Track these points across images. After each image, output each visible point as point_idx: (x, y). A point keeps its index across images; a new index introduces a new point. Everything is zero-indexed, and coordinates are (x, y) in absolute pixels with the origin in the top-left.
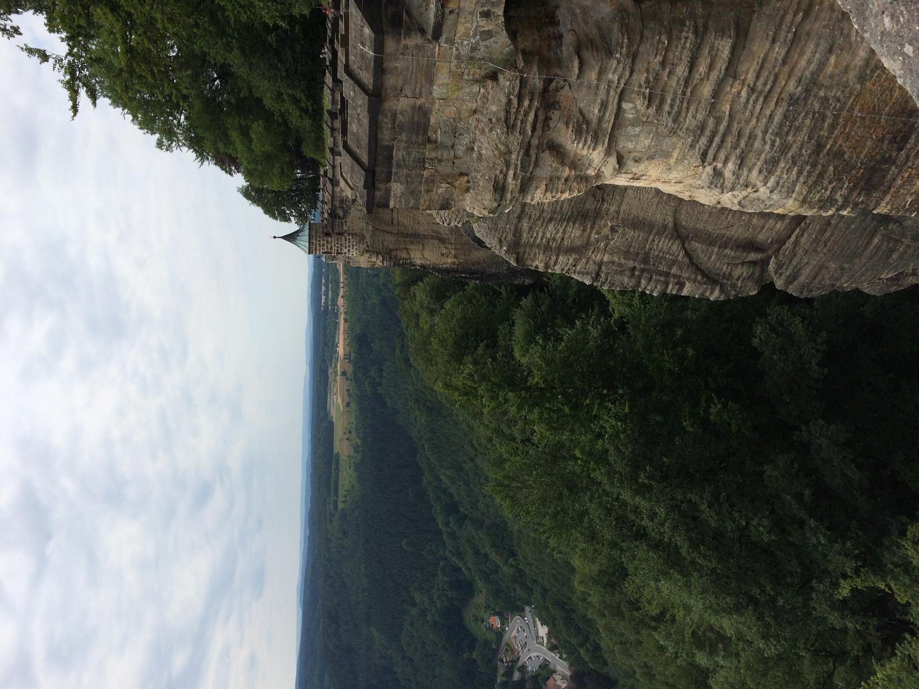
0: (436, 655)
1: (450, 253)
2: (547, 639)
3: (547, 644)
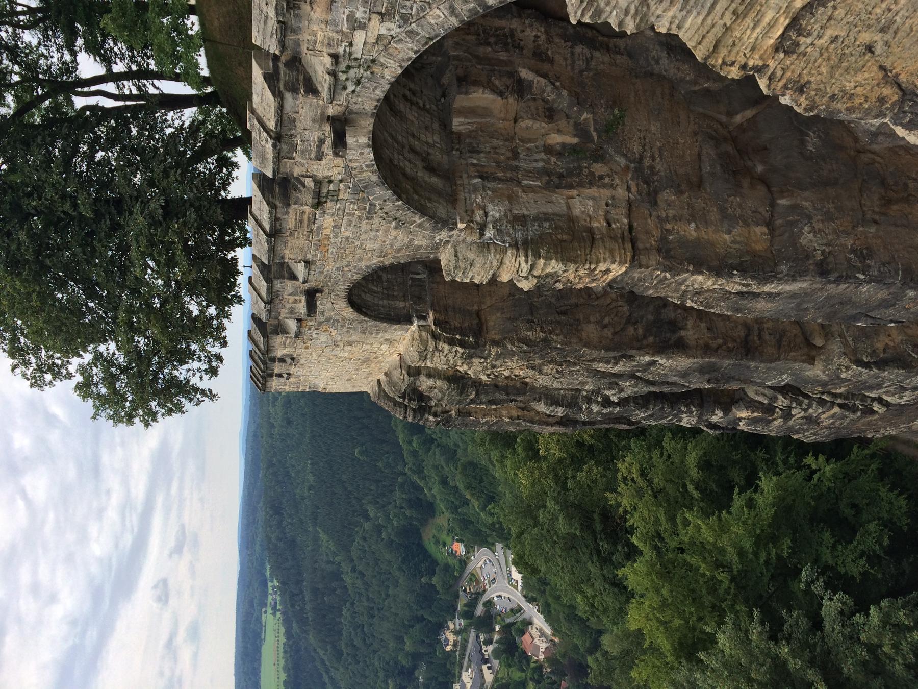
0: (390, 573)
3: (522, 590)
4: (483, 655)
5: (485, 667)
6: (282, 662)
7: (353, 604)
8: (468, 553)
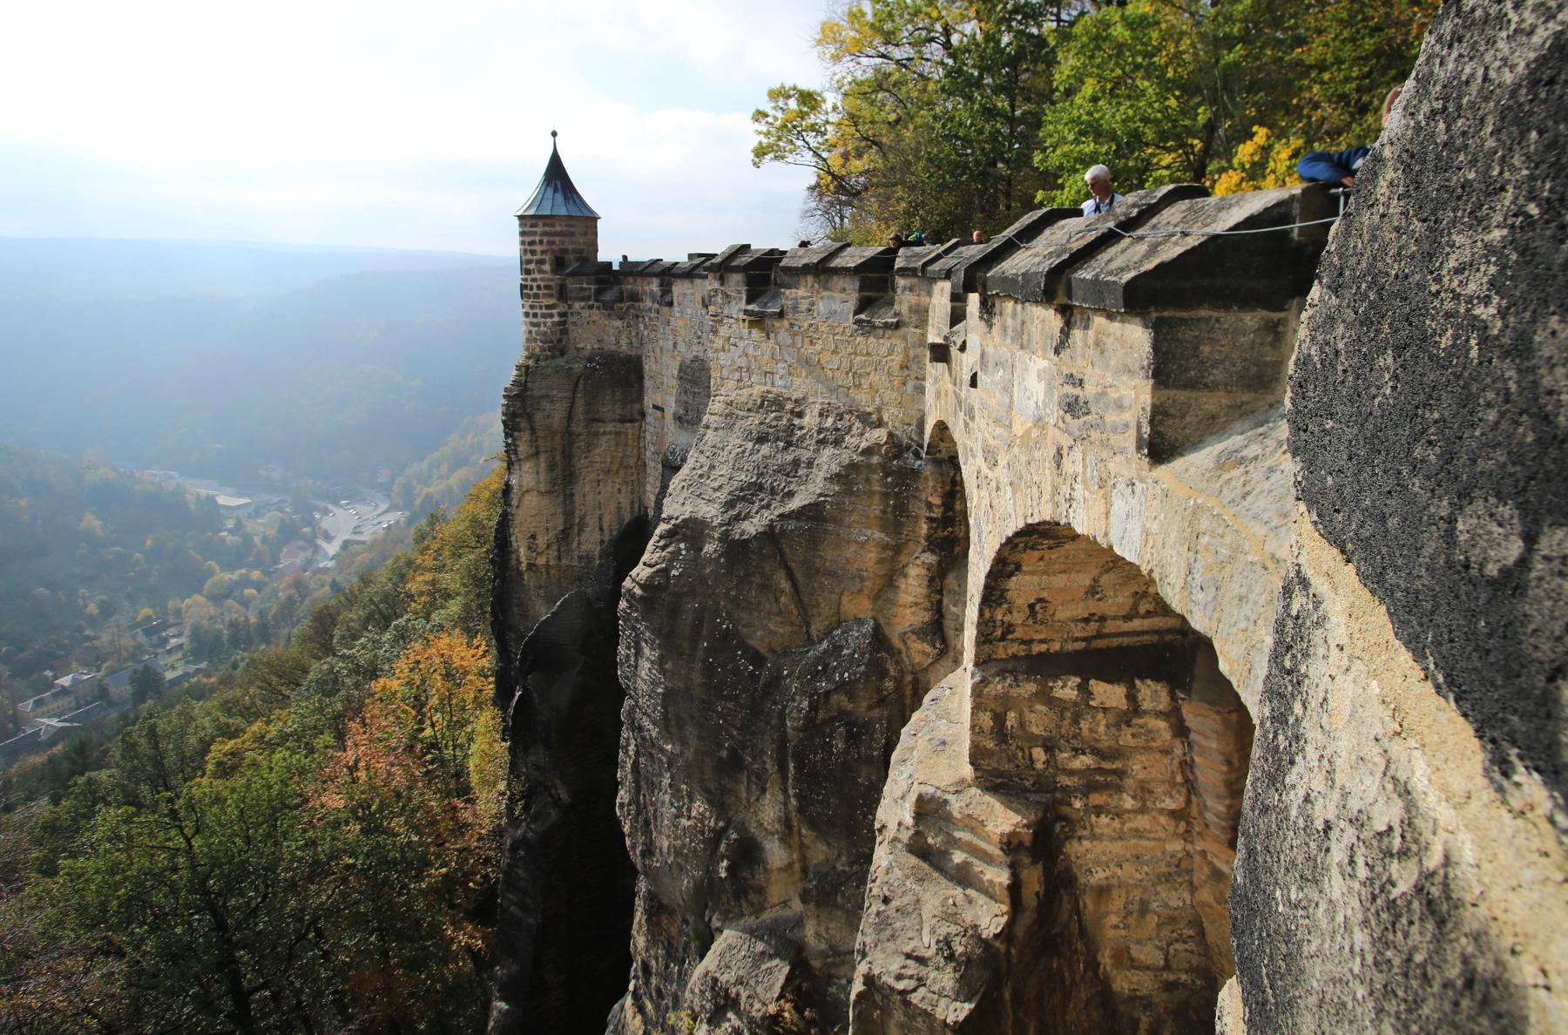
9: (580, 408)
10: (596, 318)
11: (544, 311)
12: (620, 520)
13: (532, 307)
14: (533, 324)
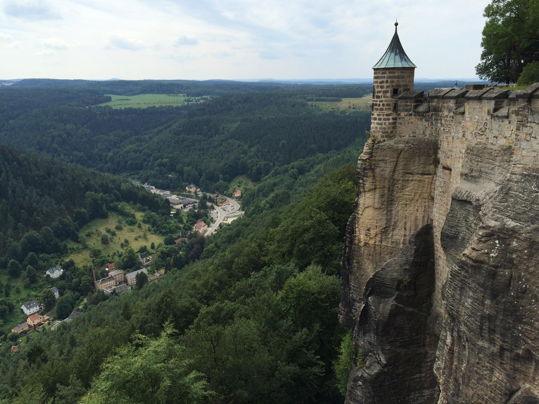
1: (371, 238)
2: (226, 223)
3: (224, 223)
4: (187, 205)
5: (182, 205)
6: (164, 105)
7: (204, 140)
8: (236, 198)
9: (400, 167)
10: (412, 120)
11: (385, 117)
12: (416, 226)
13: (378, 115)
14: (378, 124)
